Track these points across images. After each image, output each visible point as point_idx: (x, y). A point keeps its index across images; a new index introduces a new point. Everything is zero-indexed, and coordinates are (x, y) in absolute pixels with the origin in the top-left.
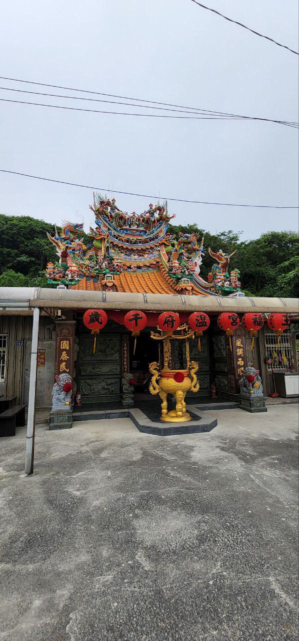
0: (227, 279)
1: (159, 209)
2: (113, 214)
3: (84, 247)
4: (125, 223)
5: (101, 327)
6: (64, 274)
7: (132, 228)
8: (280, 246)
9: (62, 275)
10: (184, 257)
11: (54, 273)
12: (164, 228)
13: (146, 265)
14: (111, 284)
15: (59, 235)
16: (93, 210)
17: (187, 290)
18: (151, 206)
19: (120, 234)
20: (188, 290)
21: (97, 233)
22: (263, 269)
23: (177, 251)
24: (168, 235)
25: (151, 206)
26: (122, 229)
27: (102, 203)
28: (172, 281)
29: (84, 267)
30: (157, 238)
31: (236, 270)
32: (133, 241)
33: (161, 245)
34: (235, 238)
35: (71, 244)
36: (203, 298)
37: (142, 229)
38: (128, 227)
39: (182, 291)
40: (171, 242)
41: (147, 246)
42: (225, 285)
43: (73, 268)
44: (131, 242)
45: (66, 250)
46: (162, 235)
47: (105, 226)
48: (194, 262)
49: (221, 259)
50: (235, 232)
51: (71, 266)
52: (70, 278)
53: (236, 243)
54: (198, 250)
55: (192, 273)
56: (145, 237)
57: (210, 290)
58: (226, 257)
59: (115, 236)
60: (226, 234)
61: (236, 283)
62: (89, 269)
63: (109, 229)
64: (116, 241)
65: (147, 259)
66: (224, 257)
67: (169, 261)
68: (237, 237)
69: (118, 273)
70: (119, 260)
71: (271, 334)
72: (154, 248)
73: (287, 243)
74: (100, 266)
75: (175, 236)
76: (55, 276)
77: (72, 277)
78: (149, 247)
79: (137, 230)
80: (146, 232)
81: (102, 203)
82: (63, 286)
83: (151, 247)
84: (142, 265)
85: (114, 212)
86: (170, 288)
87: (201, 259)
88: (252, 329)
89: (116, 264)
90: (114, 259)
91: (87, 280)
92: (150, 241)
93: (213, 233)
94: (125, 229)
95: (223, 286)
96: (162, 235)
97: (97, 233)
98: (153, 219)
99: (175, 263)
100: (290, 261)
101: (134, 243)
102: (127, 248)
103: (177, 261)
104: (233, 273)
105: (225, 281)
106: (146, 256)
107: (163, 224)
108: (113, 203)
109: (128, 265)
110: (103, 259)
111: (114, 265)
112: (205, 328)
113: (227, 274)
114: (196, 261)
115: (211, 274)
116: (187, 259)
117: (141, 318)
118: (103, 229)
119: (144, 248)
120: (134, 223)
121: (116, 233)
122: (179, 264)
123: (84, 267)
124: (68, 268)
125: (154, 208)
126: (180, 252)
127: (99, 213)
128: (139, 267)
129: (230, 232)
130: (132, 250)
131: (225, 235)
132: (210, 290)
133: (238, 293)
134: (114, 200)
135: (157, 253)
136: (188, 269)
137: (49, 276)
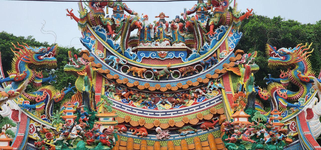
2: (118, 22)
3: (57, 94)
10: (281, 101)
12: (230, 39)
13: (189, 124)
19: (131, 62)
21: (83, 62)
30: (214, 62)
32: (161, 74)
33: (224, 76)
41: (194, 80)
46: (225, 54)
47: (101, 47)
48: (305, 109)
55: (279, 137)
56: (187, 63)
59: (120, 65)
63: (108, 53)
64: (123, 77)
65: (192, 110)
72: (207, 84)
78: (196, 84)
80: (189, 52)
83: (201, 83)
84: (180, 125)
85: (119, 18)
89: (102, 129)
90: (98, 119)
92: (199, 69)
96: (225, 54)
97: (83, 62)
99: (238, 117)
101: (161, 78)
103: (242, 113)
106: (190, 103)
109: (149, 127)
114: (310, 106)
116: (285, 104)
118: (98, 53)
119: (186, 87)
122: (249, 119)
127: (88, 22)
128: (174, 130)
130: (159, 92)
135: (215, 94)
136: (268, 129)
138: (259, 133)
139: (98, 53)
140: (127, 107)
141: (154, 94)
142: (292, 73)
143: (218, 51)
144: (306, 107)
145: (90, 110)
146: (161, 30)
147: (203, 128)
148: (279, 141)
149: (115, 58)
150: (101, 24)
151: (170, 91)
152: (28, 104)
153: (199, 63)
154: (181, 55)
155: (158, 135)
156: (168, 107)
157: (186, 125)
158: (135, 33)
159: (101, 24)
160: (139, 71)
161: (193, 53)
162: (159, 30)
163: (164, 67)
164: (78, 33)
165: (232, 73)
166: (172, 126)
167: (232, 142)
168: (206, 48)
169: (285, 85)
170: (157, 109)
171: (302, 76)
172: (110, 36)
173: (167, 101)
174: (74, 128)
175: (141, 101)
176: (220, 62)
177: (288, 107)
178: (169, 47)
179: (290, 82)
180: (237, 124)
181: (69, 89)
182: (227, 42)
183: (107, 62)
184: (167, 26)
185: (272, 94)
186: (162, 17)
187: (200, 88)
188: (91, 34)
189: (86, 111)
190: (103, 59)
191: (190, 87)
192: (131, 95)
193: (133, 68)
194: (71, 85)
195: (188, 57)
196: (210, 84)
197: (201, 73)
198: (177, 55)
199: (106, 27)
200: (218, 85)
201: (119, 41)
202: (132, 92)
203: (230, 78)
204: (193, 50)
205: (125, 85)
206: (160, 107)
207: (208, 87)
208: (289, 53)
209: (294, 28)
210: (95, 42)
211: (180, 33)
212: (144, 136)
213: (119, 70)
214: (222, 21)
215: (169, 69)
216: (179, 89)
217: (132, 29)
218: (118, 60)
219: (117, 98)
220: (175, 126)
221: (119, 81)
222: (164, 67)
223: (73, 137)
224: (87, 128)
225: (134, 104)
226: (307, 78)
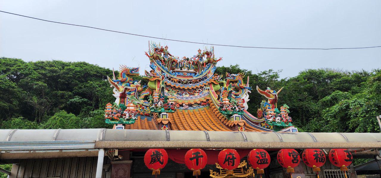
0: (278, 114)
1: (207, 54)
2: (166, 59)
4: (176, 67)
5: (161, 166)
6: (122, 114)
7: (183, 70)
8: (319, 82)
9: (119, 115)
11: (112, 113)
12: (212, 70)
13: (196, 103)
14: (166, 122)
15: (117, 79)
17: (239, 126)
18: (199, 51)
19: (172, 76)
20: (240, 126)
22: (305, 104)
23: (226, 89)
25: (199, 51)
26: (174, 72)
27: (156, 49)
28: (223, 117)
29: (139, 106)
30: (206, 78)
31: (285, 106)
32: (185, 82)
33: (210, 84)
34: (276, 76)
35: (130, 86)
36: (263, 134)
37: (192, 71)
38: (179, 70)
39: (234, 127)
40: (219, 81)
41: (198, 85)
42: (277, 120)
43: (131, 108)
44: (183, 82)
45: (125, 91)
46: (210, 75)
47: (159, 69)
49: (269, 96)
50: (275, 70)
51: (129, 106)
52: (127, 118)
53: (277, 80)
54: (244, 88)
55: (242, 109)
56: (195, 78)
57: (261, 125)
58: (274, 94)
59: (167, 77)
62: (143, 108)
64: (169, 83)
65: (198, 97)
66: (273, 94)
67: (218, 99)
68: (277, 75)
69: (173, 111)
70: (174, 99)
71: (330, 170)
72: (203, 87)
73: (325, 79)
74: (156, 105)
75: (222, 76)
76: (113, 116)
77: (130, 116)
78: (199, 87)
80: (196, 74)
81: (156, 49)
82: (121, 126)
83: (201, 87)
84: (193, 103)
85: (167, 57)
86: (222, 124)
87: (248, 96)
88: (314, 166)
89: (170, 103)
90: (168, 99)
91: (141, 119)
92: (200, 81)
94: (177, 71)
97: (152, 75)
98: (201, 62)
99: (225, 100)
100: (332, 95)
101: (185, 84)
102: (179, 88)
103: (227, 99)
105: (276, 116)
106: (196, 94)
107: (212, 66)
108: (166, 50)
109: (180, 104)
110: (158, 99)
111: (168, 104)
112: (266, 166)
113: (276, 109)
114: (243, 98)
115: (260, 110)
117: (202, 156)
118: (157, 72)
119: (195, 88)
120: (185, 66)
122: (229, 101)
123: (139, 106)
124: (126, 108)
125: (202, 52)
126: (230, 90)
127: (153, 58)
128: (190, 105)
129: (270, 71)
130: (184, 89)
131: (266, 74)
132: (261, 125)
133: (291, 128)
134: (167, 47)
135: (206, 91)
136: (238, 106)
137: (107, 116)
138: (233, 108)
141: (182, 90)
142: (236, 84)
143: (207, 74)
146: (184, 64)
147: (202, 105)
148: (241, 111)
149: (166, 74)
150: (159, 59)
151: (188, 89)
154: (193, 75)
155: (184, 107)
157: (195, 103)
159: (159, 59)
161: (197, 74)
162: (184, 64)
163: (186, 79)
165: (213, 83)
166: (190, 103)
167: (223, 110)
168: (202, 72)
171: (241, 85)
173: (187, 93)
174: (159, 102)
175: (176, 93)
176: (208, 78)
178: (188, 71)
179: (235, 88)
181: (145, 86)
187: (200, 88)
188: (155, 63)
190: (160, 74)
191: (197, 88)
193: (173, 79)
194: (146, 85)
195: (195, 75)
196: (204, 87)
197: (201, 82)
198: (191, 74)
199: (161, 61)
200: (208, 87)
206: (184, 96)
207: (204, 88)
208: (235, 76)
210: (157, 66)
211: (192, 65)
212: (178, 107)
213: (167, 79)
215: (188, 80)
218: (167, 75)
220: (191, 104)
221: (168, 84)
222: (186, 79)
223: (159, 106)
226: (243, 87)
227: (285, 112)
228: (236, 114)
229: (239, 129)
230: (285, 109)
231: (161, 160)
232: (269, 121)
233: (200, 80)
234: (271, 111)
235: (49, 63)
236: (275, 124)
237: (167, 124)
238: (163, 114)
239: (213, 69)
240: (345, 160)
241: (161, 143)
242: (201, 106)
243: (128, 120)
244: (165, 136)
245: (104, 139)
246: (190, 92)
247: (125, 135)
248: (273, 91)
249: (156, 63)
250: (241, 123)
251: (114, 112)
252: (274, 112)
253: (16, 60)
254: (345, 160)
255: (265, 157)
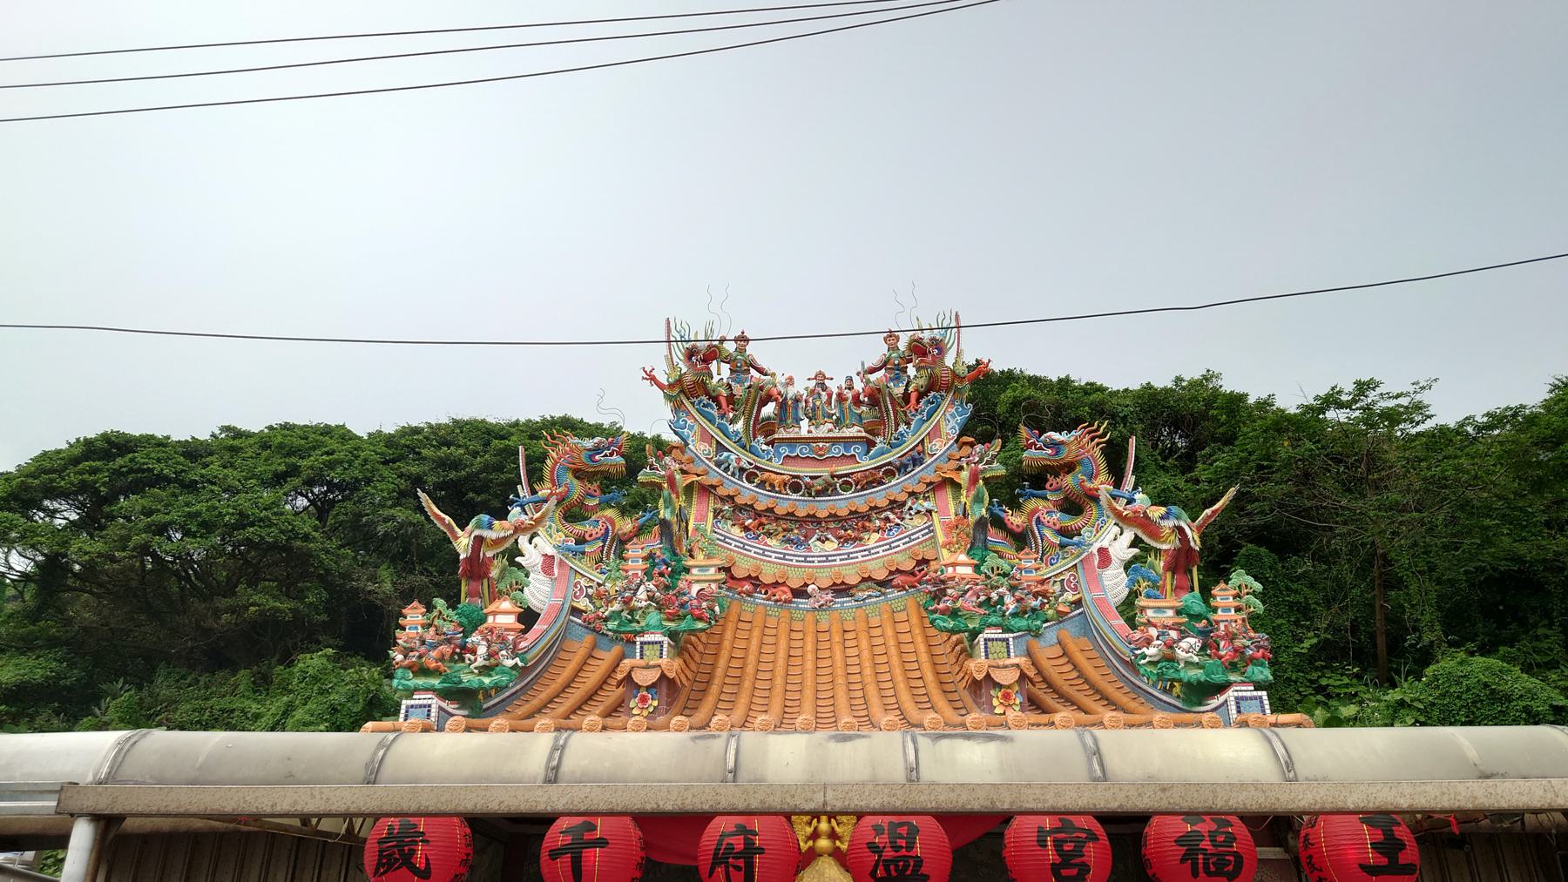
0: (1190, 621)
1: (918, 348)
2: (738, 390)
10: (1048, 533)
12: (951, 417)
13: (870, 579)
14: (651, 677)
15: (534, 492)
16: (660, 386)
20: (1000, 686)
24: (965, 443)
27: (690, 354)
30: (917, 461)
31: (1240, 577)
33: (936, 487)
36: (833, 745)
41: (879, 496)
42: (1181, 654)
46: (939, 447)
47: (706, 437)
48: (1094, 549)
52: (480, 662)
55: (1035, 603)
56: (866, 464)
59: (742, 470)
60: (1344, 398)
61: (1238, 643)
63: (721, 447)
64: (747, 491)
65: (878, 552)
72: (904, 504)
77: (490, 655)
78: (882, 502)
79: (834, 441)
80: (871, 444)
83: (892, 502)
85: (741, 382)
89: (695, 588)
90: (687, 570)
93: (1290, 402)
95: (1171, 659)
96: (939, 447)
99: (954, 565)
101: (819, 493)
103: (963, 558)
104: (1223, 595)
105: (1183, 635)
108: (741, 351)
109: (796, 584)
113: (1192, 600)
114: (1105, 544)
116: (1056, 540)
117: (601, 842)
118: (699, 448)
119: (864, 508)
121: (746, 459)
122: (977, 568)
124: (483, 620)
127: (682, 391)
128: (841, 589)
130: (813, 519)
133: (1231, 694)
135: (919, 522)
136: (1012, 589)
138: (994, 596)
139: (699, 448)
140: (754, 549)
142: (1069, 480)
144: (1097, 546)
145: (675, 554)
148: (1034, 610)
149: (733, 457)
152: (571, 543)
153: (890, 463)
156: (831, 546)
157: (864, 580)
158: (769, 410)
159: (707, 393)
160: (777, 480)
163: (824, 472)
164: (666, 411)
167: (943, 612)
169: (1055, 504)
170: (809, 549)
171: (1088, 485)
172: (722, 416)
175: (780, 537)
177: (1062, 546)
179: (1066, 498)
180: (952, 579)
181: (648, 515)
182: (943, 424)
183: (718, 464)
184: (830, 396)
185: (1030, 521)
186: (821, 379)
187: (891, 510)
189: (667, 556)
191: (871, 509)
192: (761, 524)
199: (716, 399)
201: (740, 426)
202: (764, 520)
203: (949, 492)
204: (878, 440)
205: (751, 506)
208: (1062, 443)
209: (1095, 397)
213: (740, 479)
214: (933, 385)
216: (851, 513)
217: (764, 403)
218: (739, 460)
219: (737, 532)
221: (739, 500)
224: (667, 587)
225: (769, 541)
227: (1238, 609)
228: (996, 626)
229: (995, 702)
230: (1235, 597)
231: (419, 861)
232: (1144, 656)
233: (891, 471)
234: (1158, 609)
235: (435, 429)
236: (1171, 673)
237: (654, 685)
238: (647, 638)
239: (953, 416)
240: (1362, 867)
241: (317, 793)
242: (893, 594)
243: (485, 670)
244: (366, 757)
245: (111, 777)
246: (843, 528)
247: (201, 759)
248: (1163, 510)
249: (693, 412)
250: (1004, 672)
251: (428, 640)
252: (1178, 612)
253: (327, 431)
254: (1362, 867)
255: (910, 846)
